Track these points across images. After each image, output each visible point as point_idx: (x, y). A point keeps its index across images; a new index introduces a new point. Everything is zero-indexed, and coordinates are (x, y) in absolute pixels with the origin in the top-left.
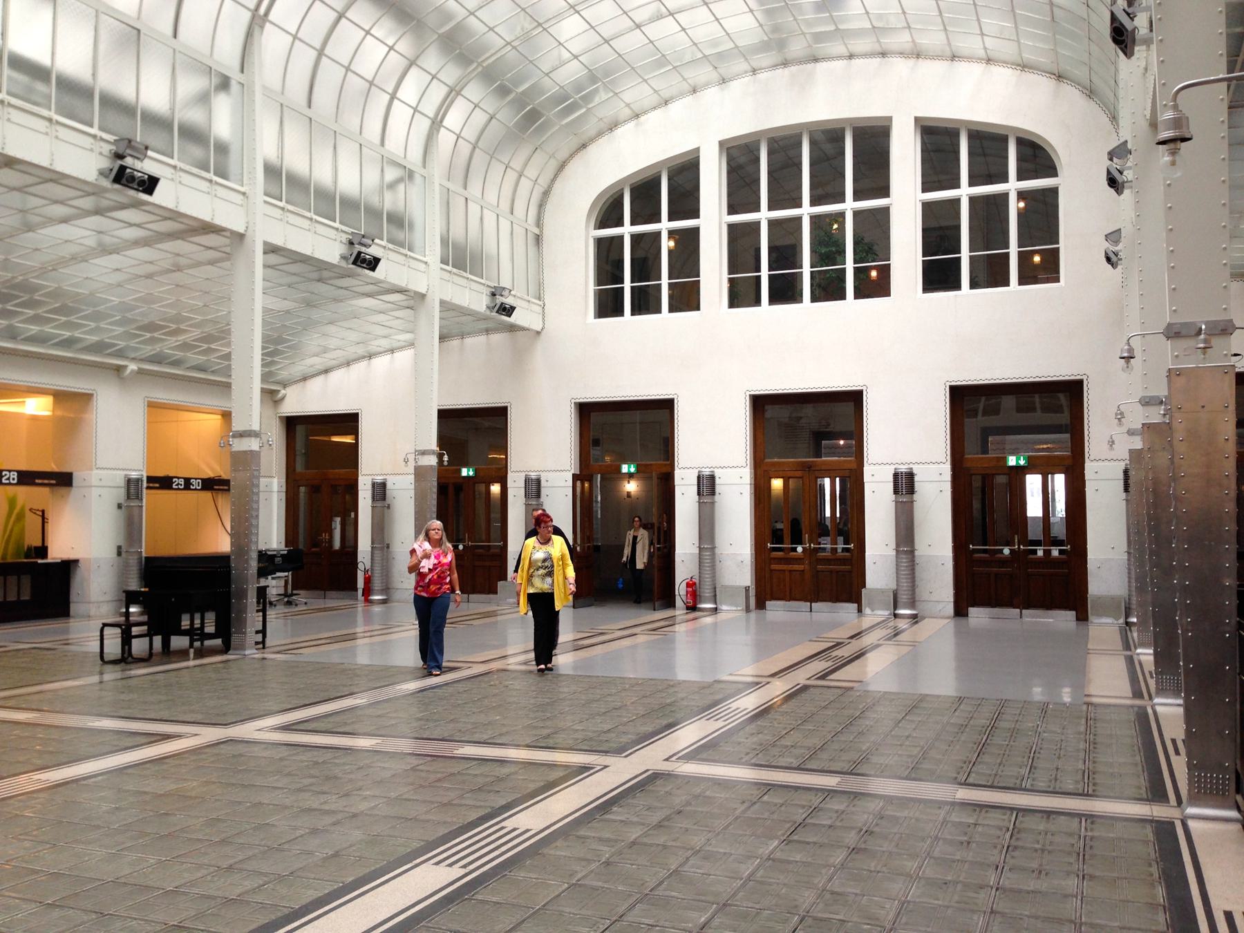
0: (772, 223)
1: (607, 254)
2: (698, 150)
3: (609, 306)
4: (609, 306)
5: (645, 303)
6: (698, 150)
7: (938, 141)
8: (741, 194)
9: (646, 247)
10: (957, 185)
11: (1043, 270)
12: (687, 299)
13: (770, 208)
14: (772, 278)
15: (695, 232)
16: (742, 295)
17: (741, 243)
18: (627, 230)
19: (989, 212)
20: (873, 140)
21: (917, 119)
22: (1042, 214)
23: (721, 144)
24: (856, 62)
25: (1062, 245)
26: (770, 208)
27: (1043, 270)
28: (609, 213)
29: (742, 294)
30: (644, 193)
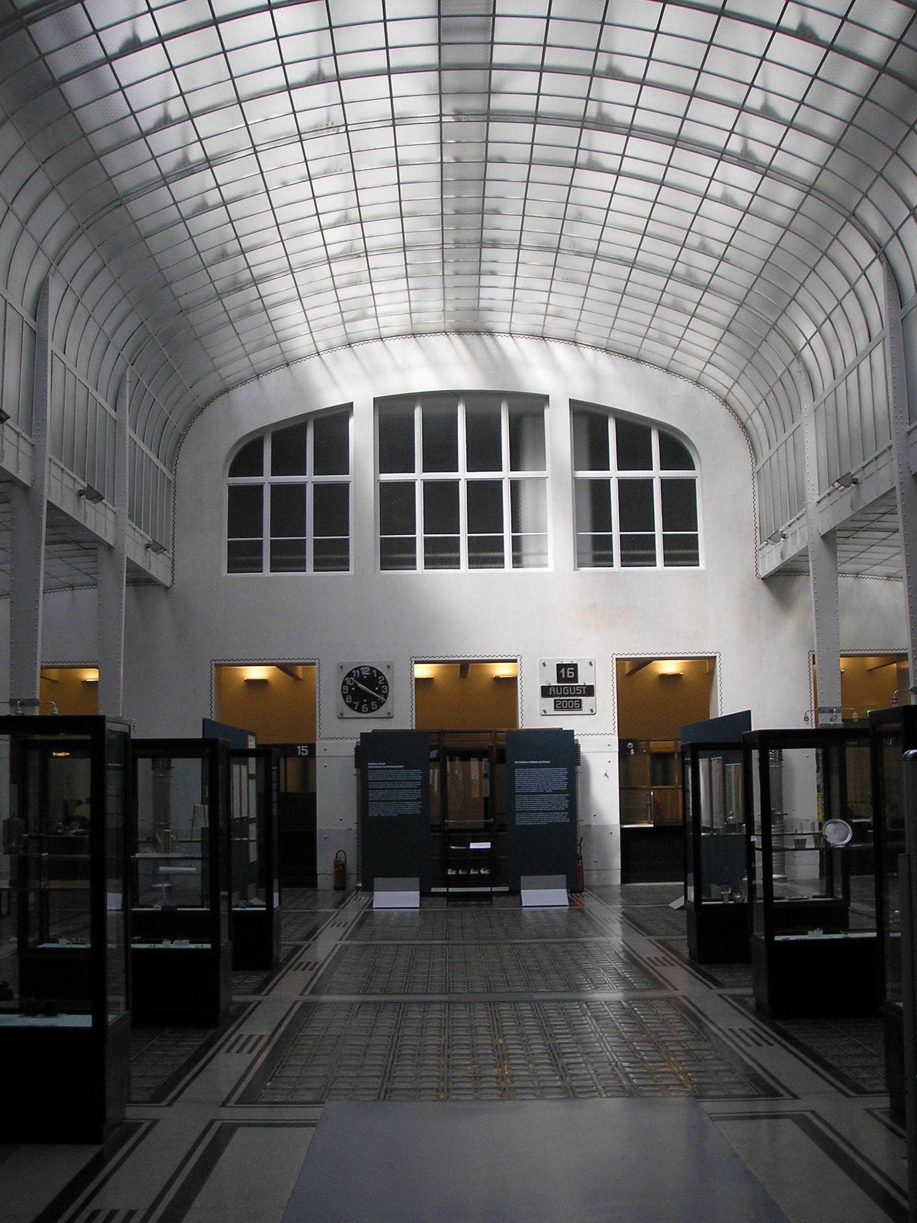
0: (428, 486)
1: (243, 505)
2: (352, 404)
3: (243, 558)
4: (243, 558)
5: (288, 558)
6: (352, 404)
8: (394, 453)
9: (287, 499)
11: (683, 551)
13: (425, 470)
14: (426, 540)
15: (344, 488)
17: (394, 501)
18: (267, 479)
19: (636, 495)
21: (572, 402)
22: (681, 500)
25: (700, 532)
26: (425, 470)
27: (683, 551)
28: (246, 458)
29: (395, 555)
30: (287, 441)
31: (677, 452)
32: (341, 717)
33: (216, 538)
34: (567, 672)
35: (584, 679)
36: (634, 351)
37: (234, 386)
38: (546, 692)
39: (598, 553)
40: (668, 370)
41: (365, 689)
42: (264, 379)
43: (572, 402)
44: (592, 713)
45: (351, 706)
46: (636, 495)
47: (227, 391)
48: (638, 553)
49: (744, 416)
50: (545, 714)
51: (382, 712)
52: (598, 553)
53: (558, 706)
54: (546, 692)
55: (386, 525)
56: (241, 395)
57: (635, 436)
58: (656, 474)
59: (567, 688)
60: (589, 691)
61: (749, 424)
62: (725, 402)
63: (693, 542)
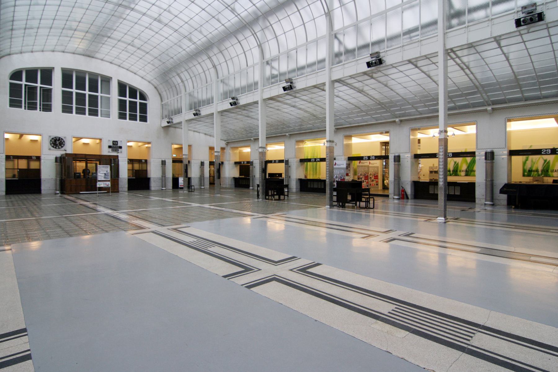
6: (54, 68)
7: (122, 87)
10: (130, 98)
11: (144, 119)
12: (47, 108)
15: (50, 90)
16: (67, 109)
19: (133, 105)
20: (107, 80)
21: (118, 80)
22: (144, 108)
23: (62, 68)
24: (103, 62)
27: (144, 119)
29: (67, 109)
30: (31, 74)
31: (143, 97)
32: (50, 149)
33: (6, 98)
34: (115, 143)
35: (119, 145)
36: (135, 72)
37: (13, 54)
38: (110, 147)
39: (122, 116)
40: (142, 78)
41: (57, 143)
42: (24, 54)
43: (118, 80)
44: (121, 152)
45: (53, 147)
46: (133, 105)
47: (10, 55)
48: (133, 118)
49: (160, 92)
50: (109, 152)
51: (63, 149)
52: (122, 116)
53: (113, 151)
54: (110, 147)
55: (64, 101)
56: (15, 57)
57: (133, 92)
58: (138, 101)
59: (115, 146)
60: (121, 147)
61: (162, 94)
62: (155, 88)
63: (146, 117)
